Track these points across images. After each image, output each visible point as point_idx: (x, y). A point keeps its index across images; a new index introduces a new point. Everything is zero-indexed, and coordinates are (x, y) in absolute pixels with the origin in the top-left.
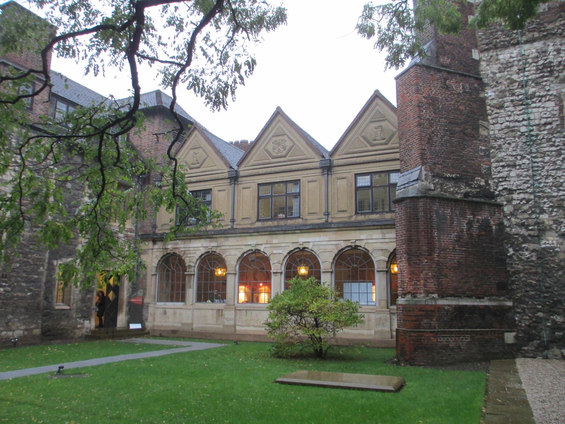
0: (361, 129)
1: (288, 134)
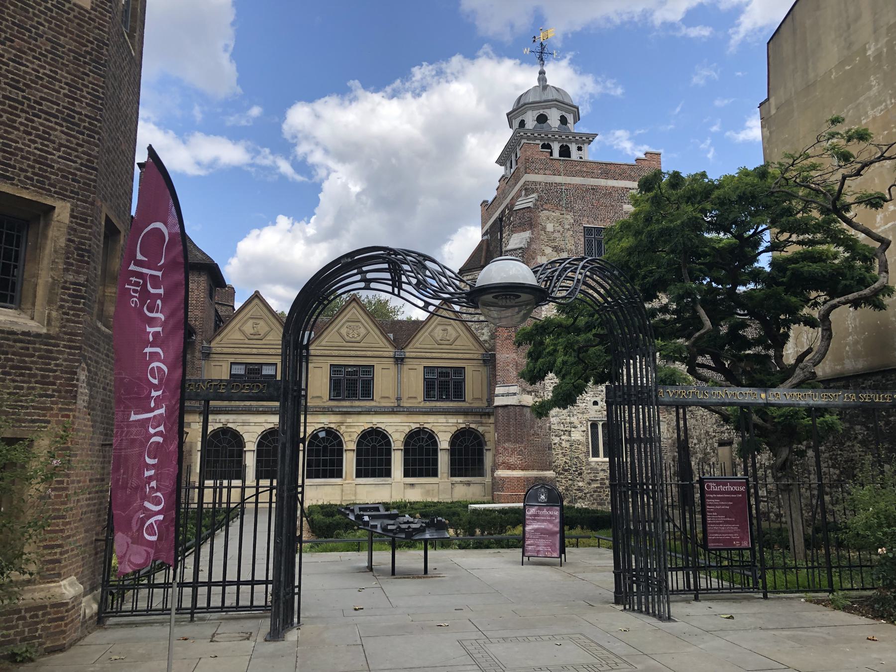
1: (363, 321)
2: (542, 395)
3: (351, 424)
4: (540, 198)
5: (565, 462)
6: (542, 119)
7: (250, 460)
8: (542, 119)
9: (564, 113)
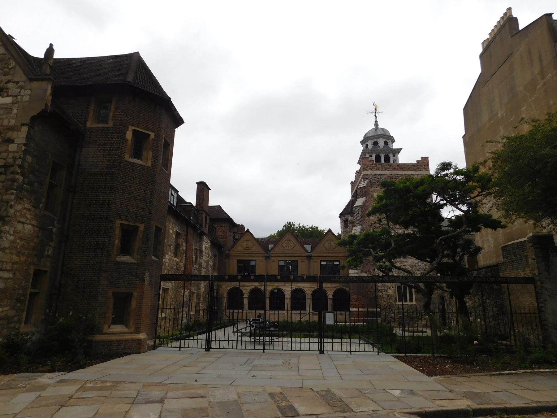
0: (323, 243)
1: (293, 240)
2: (373, 273)
3: (289, 287)
4: (370, 182)
5: (385, 304)
6: (376, 143)
7: (246, 301)
8: (376, 143)
9: (386, 140)
